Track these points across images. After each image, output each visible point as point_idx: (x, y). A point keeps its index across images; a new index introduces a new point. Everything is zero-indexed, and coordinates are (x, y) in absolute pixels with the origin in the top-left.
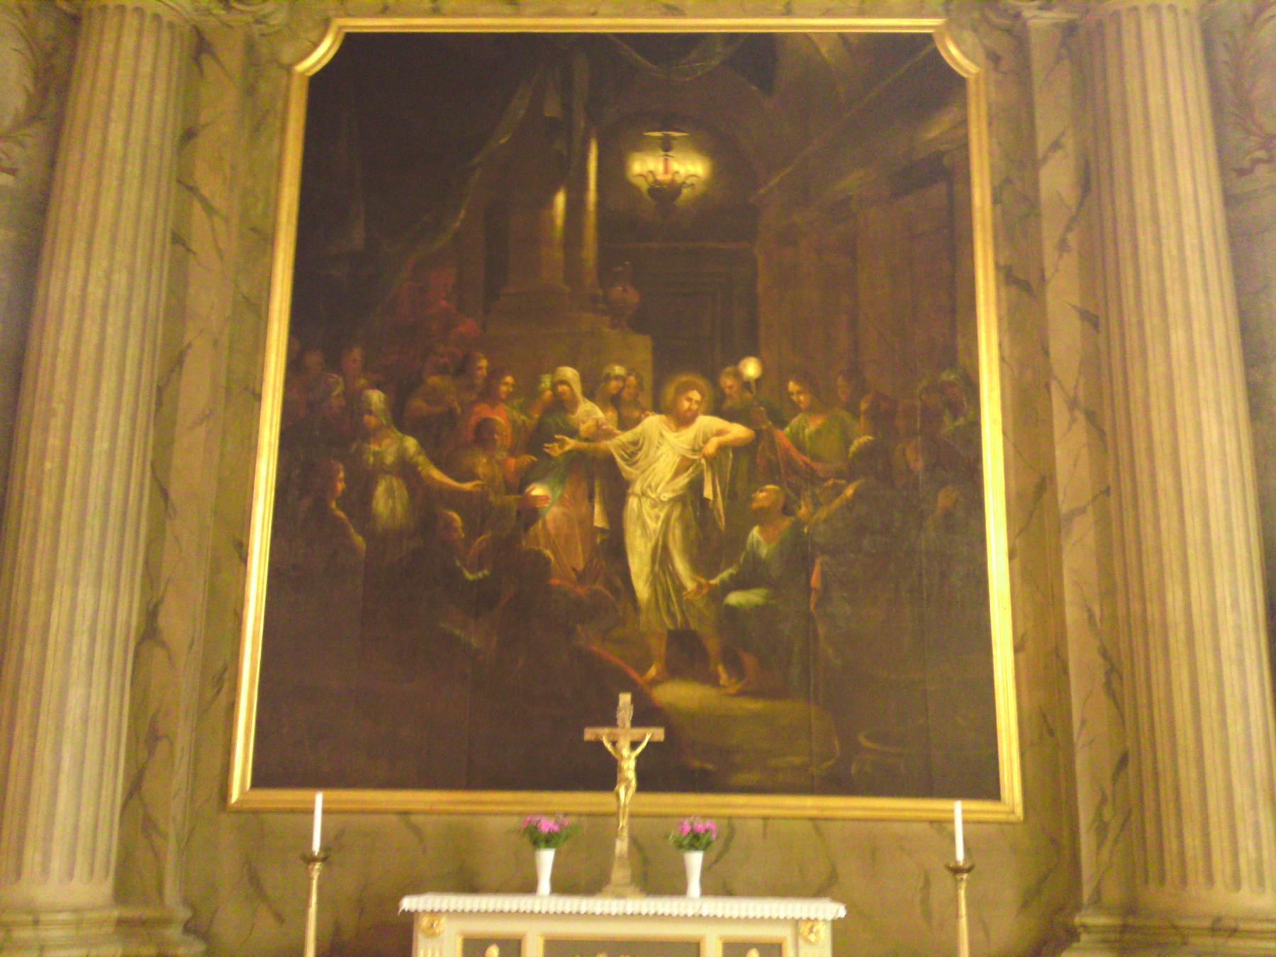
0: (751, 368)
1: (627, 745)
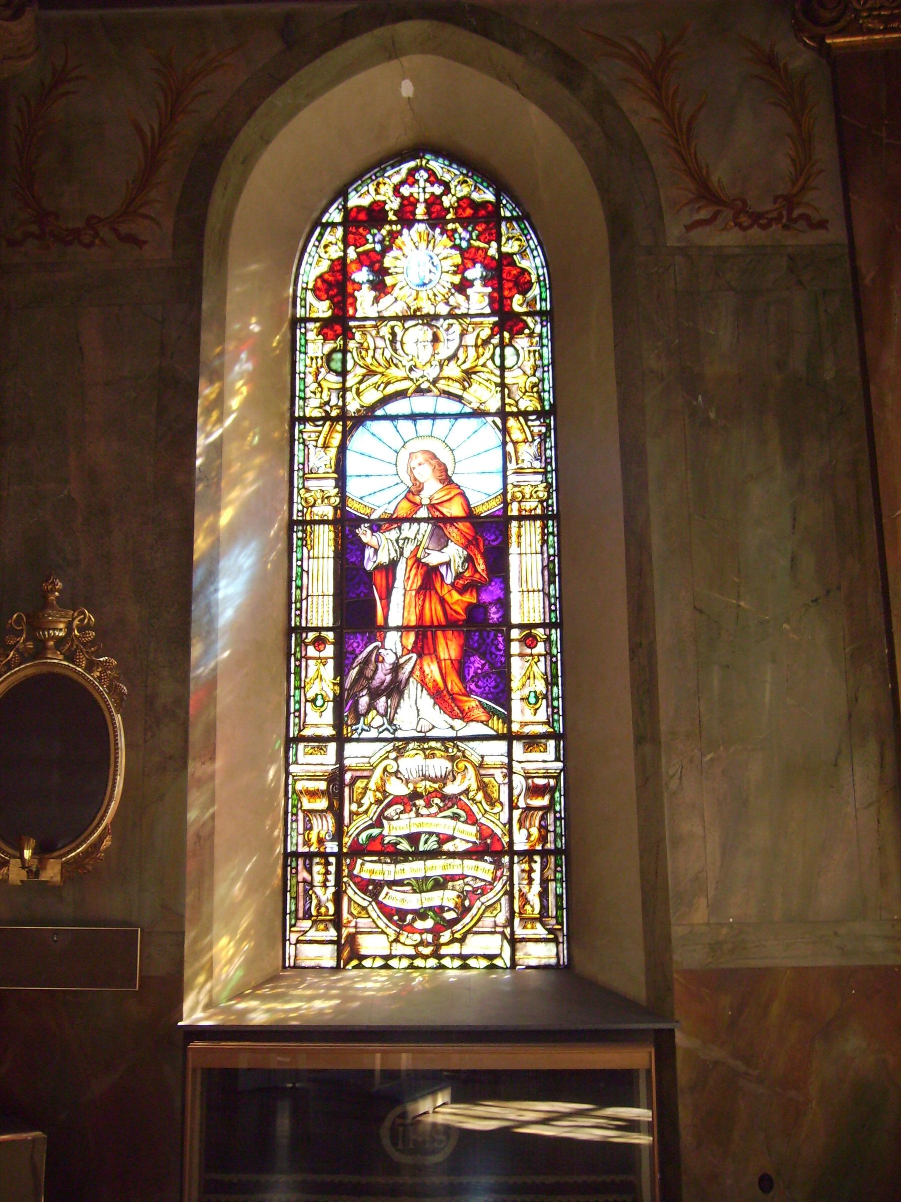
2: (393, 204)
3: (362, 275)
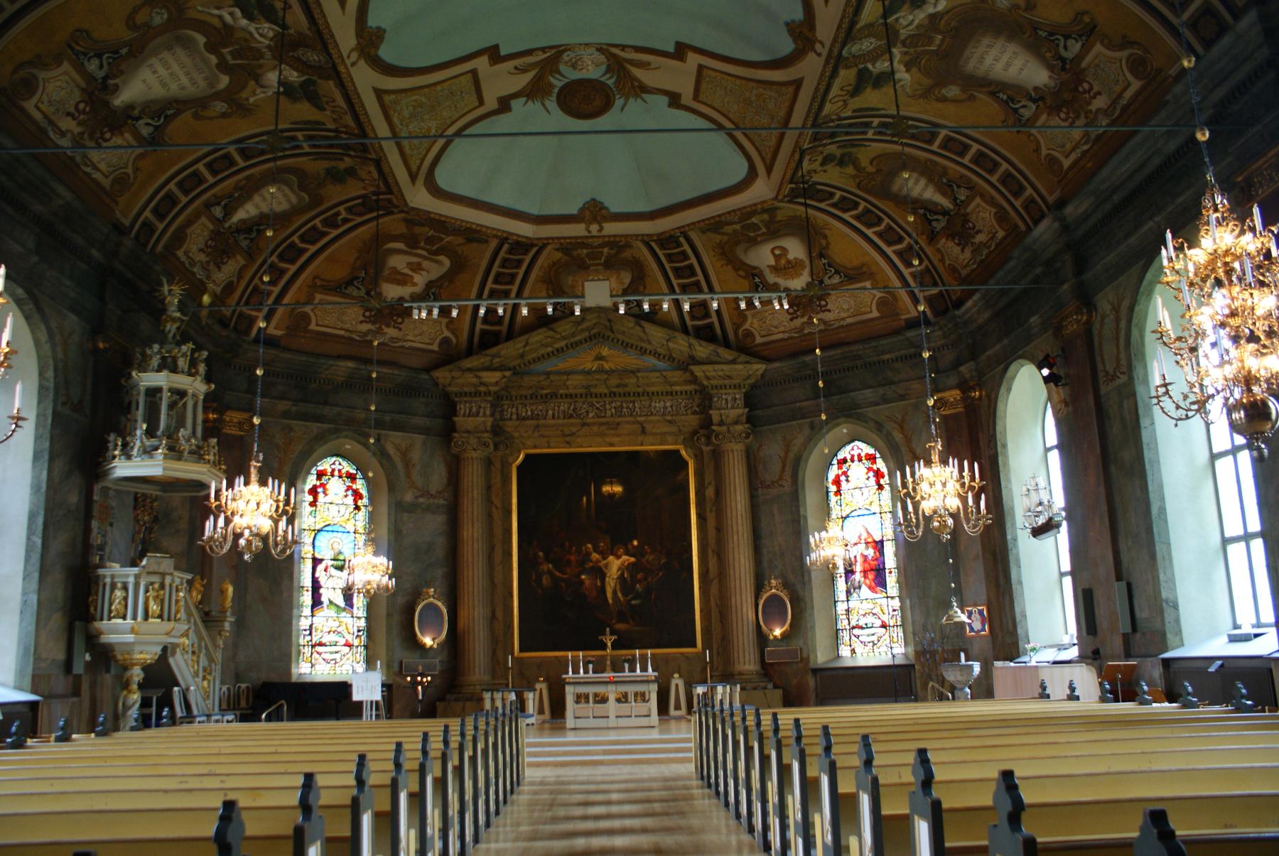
0: (635, 543)
1: (609, 640)
2: (329, 470)
3: (320, 490)
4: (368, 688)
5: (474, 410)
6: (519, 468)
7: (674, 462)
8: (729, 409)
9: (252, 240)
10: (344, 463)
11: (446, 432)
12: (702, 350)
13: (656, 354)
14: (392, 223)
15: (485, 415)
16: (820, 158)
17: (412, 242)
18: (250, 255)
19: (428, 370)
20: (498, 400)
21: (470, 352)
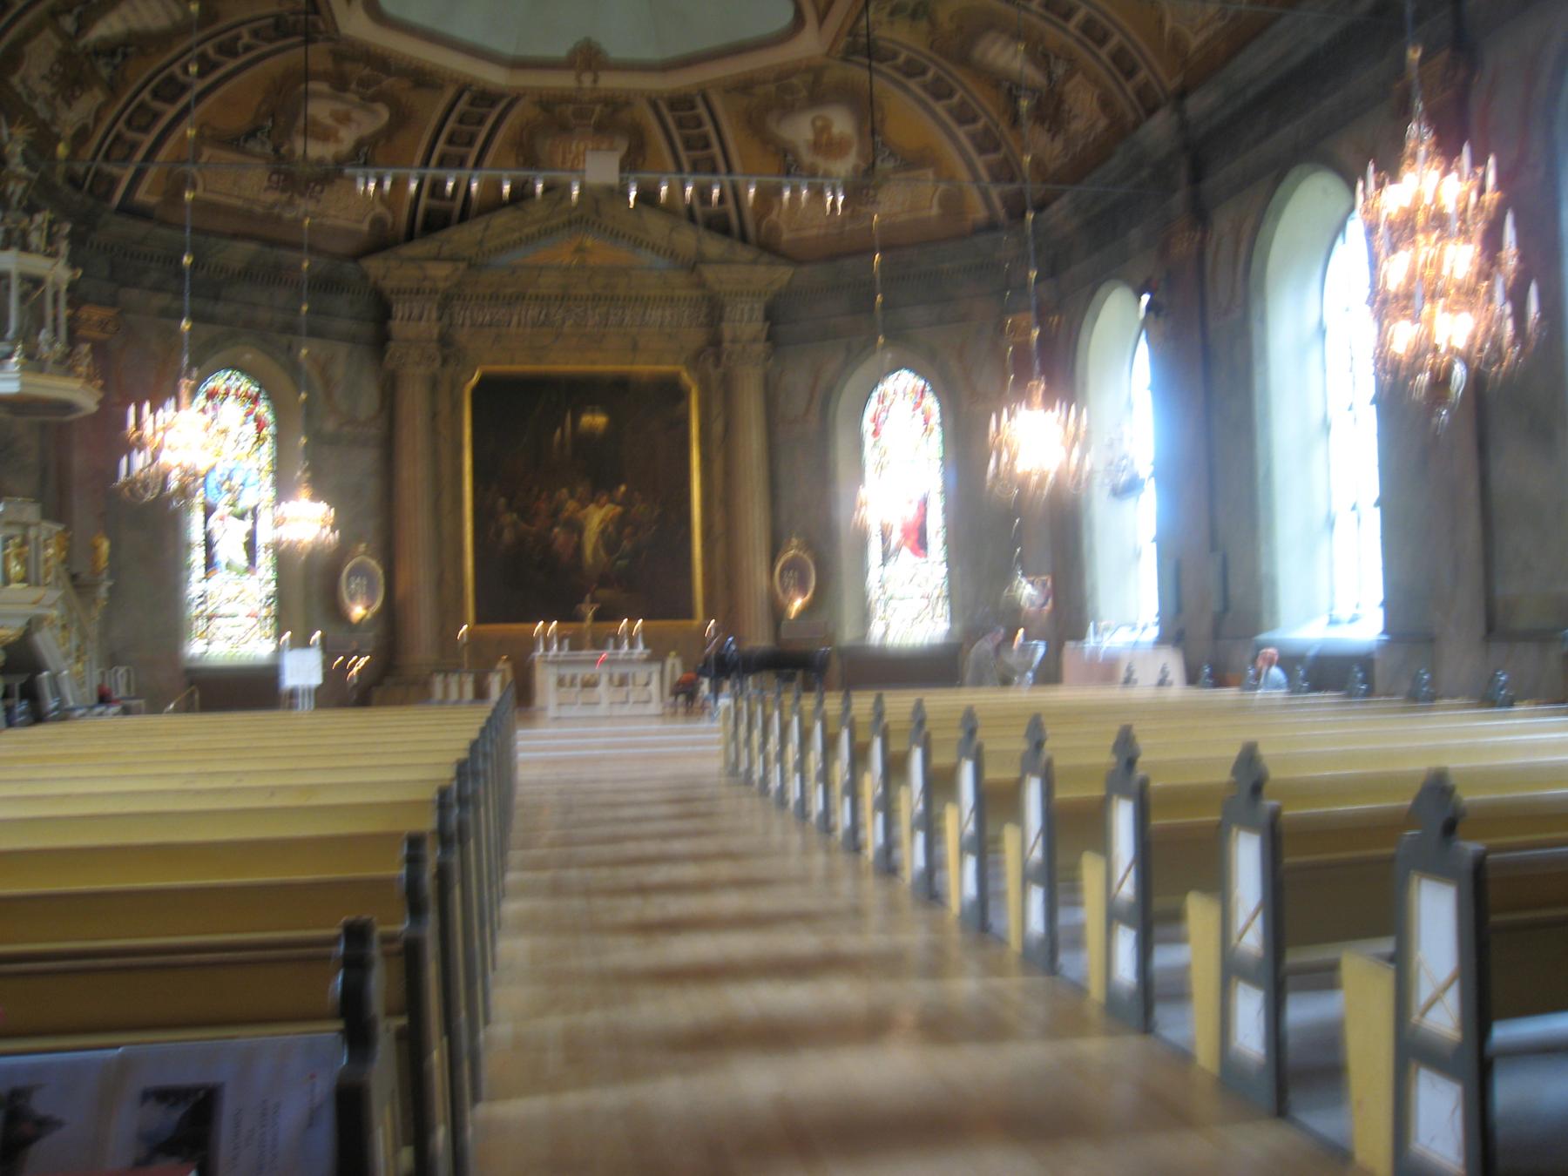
4: (303, 670)
5: (416, 312)
6: (476, 392)
7: (671, 391)
8: (744, 323)
9: (115, 68)
10: (243, 379)
11: (380, 341)
12: (714, 246)
13: (654, 248)
14: (319, 56)
15: (429, 319)
16: (888, 10)
17: (340, 84)
18: (113, 90)
19: (357, 257)
20: (446, 302)
21: (410, 236)
